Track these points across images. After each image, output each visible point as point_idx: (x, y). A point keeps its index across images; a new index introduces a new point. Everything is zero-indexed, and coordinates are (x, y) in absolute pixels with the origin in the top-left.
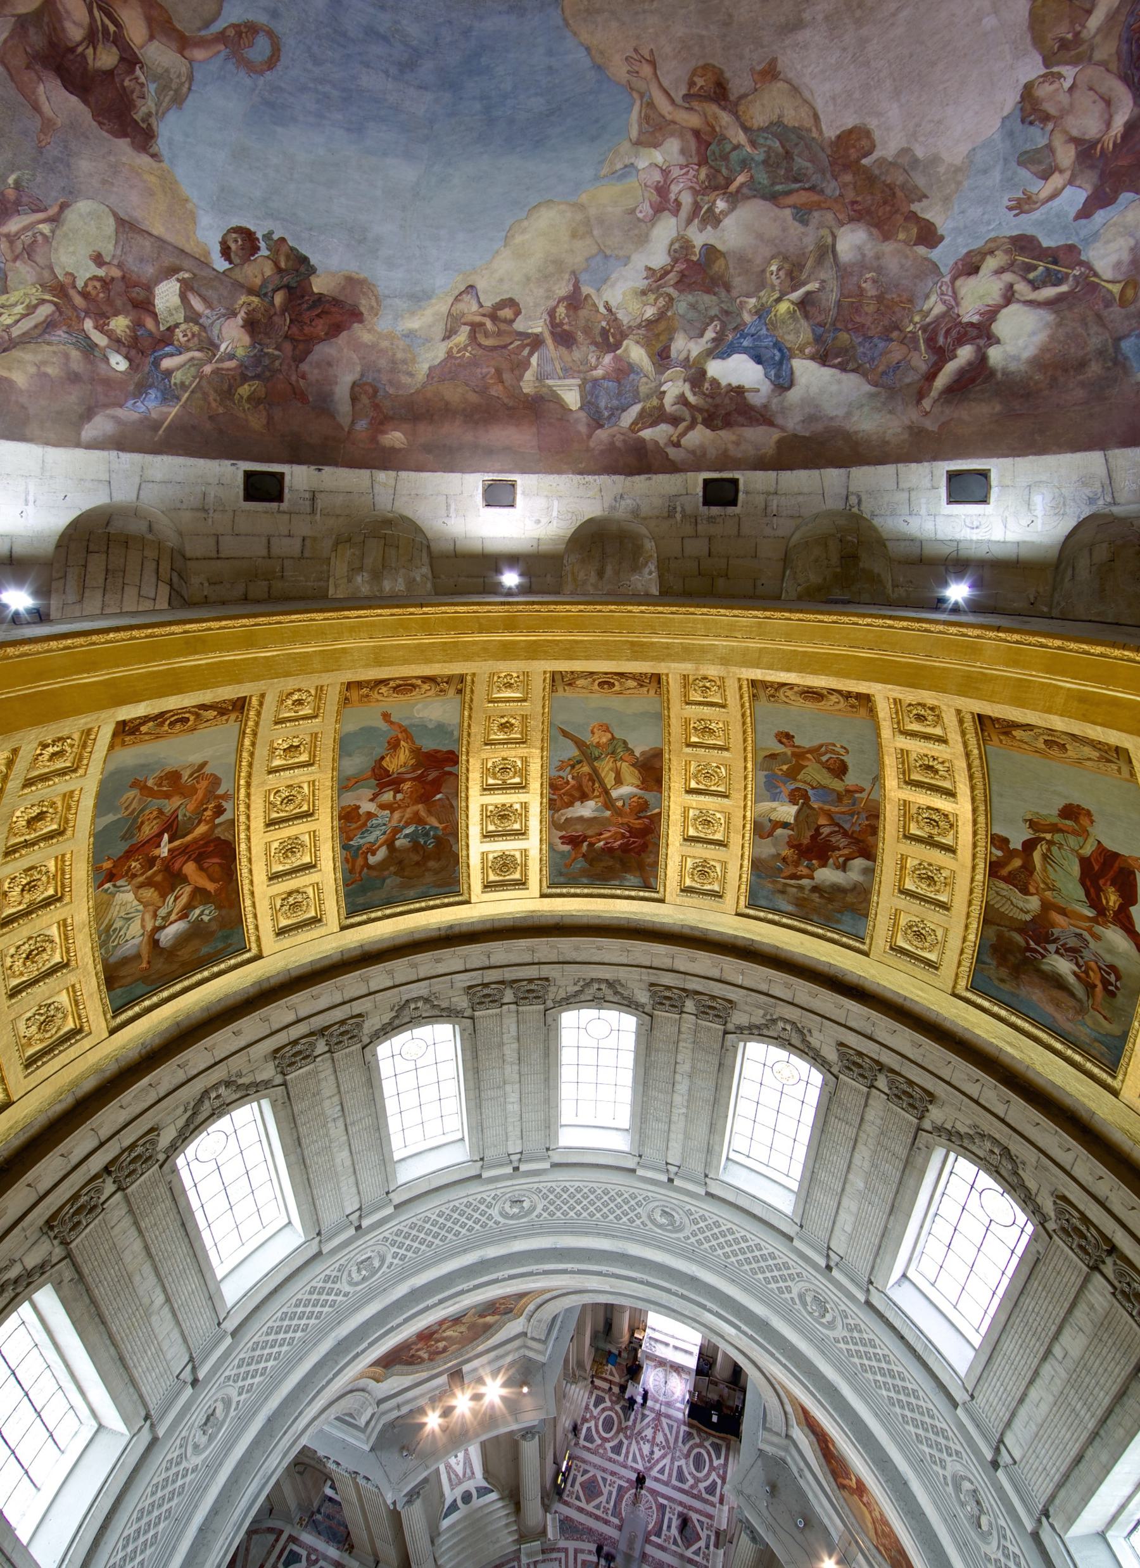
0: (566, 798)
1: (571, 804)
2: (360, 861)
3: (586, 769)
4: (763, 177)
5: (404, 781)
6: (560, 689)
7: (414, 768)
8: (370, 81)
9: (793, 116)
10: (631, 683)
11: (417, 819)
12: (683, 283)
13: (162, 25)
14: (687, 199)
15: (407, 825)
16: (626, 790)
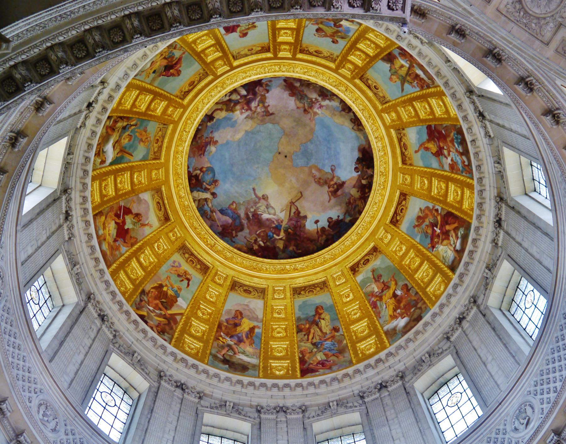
0: (423, 82)
1: (423, 79)
2: (467, 168)
3: (408, 78)
4: (306, 98)
5: (439, 145)
6: (388, 99)
7: (435, 141)
8: (333, 153)
9: (298, 102)
10: (370, 82)
11: (452, 141)
12: (326, 96)
13: (332, 180)
14: (318, 104)
15: (454, 146)
16: (402, 61)
